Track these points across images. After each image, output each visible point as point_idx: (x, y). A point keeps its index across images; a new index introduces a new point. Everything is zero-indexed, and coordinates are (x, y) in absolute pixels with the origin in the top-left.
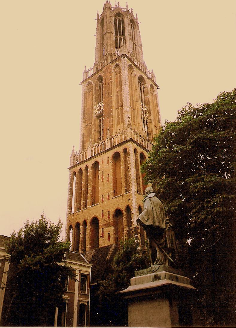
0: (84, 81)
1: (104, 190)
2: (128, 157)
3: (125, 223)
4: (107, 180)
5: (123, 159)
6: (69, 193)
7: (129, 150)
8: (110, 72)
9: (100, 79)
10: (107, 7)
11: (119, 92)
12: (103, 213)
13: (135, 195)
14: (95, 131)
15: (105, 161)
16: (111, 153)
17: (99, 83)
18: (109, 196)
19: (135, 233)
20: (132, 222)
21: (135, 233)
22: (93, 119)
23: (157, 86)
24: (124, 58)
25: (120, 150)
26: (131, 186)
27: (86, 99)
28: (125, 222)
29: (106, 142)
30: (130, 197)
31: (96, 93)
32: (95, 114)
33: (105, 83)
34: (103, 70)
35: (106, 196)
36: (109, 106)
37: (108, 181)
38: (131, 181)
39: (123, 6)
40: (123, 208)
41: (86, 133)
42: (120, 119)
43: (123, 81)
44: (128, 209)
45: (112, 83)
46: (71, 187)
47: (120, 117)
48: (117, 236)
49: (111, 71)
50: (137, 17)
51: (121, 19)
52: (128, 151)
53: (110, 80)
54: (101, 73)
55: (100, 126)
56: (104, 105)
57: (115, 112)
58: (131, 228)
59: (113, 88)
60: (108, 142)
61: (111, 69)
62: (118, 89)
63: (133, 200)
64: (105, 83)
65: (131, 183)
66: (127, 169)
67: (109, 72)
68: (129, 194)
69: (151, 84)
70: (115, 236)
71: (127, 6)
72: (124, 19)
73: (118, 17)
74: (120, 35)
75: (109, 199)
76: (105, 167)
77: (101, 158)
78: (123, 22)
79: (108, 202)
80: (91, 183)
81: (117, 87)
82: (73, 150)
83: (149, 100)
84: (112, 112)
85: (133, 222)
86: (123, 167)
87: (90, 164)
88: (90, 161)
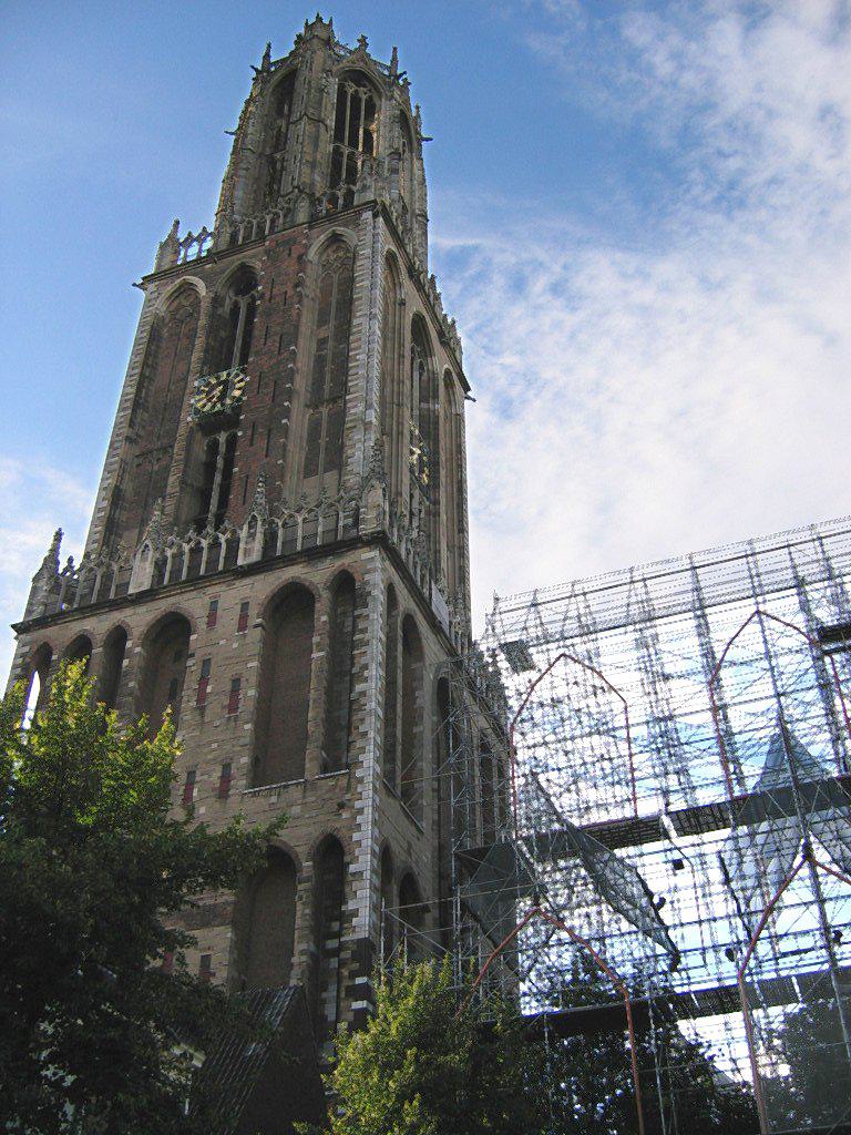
0: (159, 276)
1: (206, 750)
2: (356, 613)
3: (304, 915)
4: (227, 702)
5: (324, 618)
7: (367, 583)
8: (300, 258)
9: (244, 280)
10: (316, 36)
11: (331, 343)
13: (375, 790)
14: (183, 482)
15: (228, 619)
16: (260, 588)
17: (231, 293)
18: (226, 778)
19: (356, 966)
20: (346, 918)
21: (356, 966)
22: (182, 430)
23: (467, 388)
24: (375, 216)
25: (318, 575)
26: (359, 744)
27: (158, 347)
28: (302, 913)
29: (243, 534)
30: (348, 796)
31: (211, 331)
32: (197, 411)
33: (267, 296)
34: (267, 243)
36: (276, 387)
38: (362, 720)
39: (380, 55)
40: (300, 838)
41: (128, 487)
42: (322, 450)
43: (360, 298)
44: (333, 851)
45: (305, 301)
47: (323, 441)
48: (243, 977)
49: (306, 254)
50: (418, 116)
51: (364, 97)
52: (358, 585)
53: (297, 286)
54: (256, 259)
57: (298, 419)
58: (332, 944)
59: (303, 320)
60: (252, 536)
61: (307, 247)
62: (327, 331)
63: (360, 812)
64: (267, 296)
65: (362, 729)
66: (343, 670)
67: (294, 255)
68: (344, 781)
69: (446, 366)
70: (236, 975)
71: (394, 60)
72: (376, 99)
75: (223, 793)
76: (222, 642)
77: (207, 600)
78: (371, 110)
79: (217, 805)
80: (134, 707)
81: (322, 322)
82: (55, 551)
83: (437, 423)
84: (287, 413)
85: (355, 913)
86: (322, 654)
87: (138, 620)
88: (142, 609)
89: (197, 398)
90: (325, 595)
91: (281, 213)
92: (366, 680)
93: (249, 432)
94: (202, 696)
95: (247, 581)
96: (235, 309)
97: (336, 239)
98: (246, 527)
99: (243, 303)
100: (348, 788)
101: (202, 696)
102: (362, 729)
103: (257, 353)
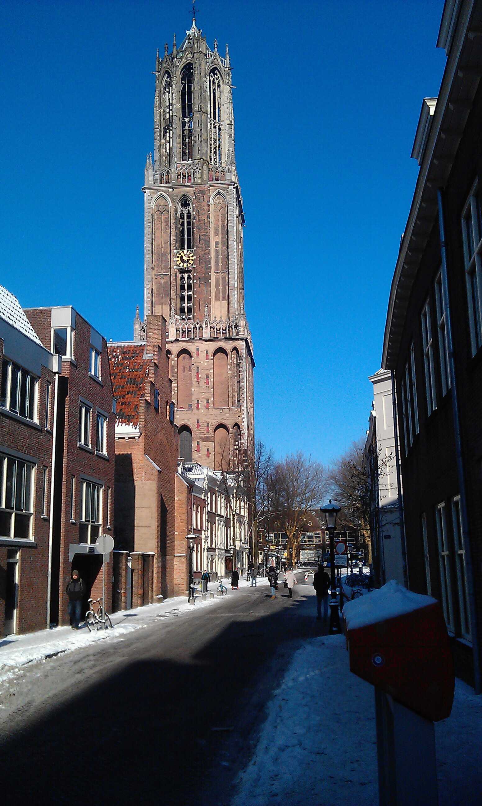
12: (198, 423)
15: (203, 355)
16: (213, 346)
25: (228, 346)
29: (204, 326)
35: (203, 403)
37: (207, 383)
40: (229, 423)
55: (182, 287)
56: (195, 257)
62: (219, 239)
74: (215, 118)
75: (208, 408)
79: (206, 410)
81: (216, 234)
88: (175, 345)
89: (177, 259)
94: (198, 378)
95: (207, 343)
96: (182, 214)
97: (219, 193)
99: (185, 212)
101: (198, 378)
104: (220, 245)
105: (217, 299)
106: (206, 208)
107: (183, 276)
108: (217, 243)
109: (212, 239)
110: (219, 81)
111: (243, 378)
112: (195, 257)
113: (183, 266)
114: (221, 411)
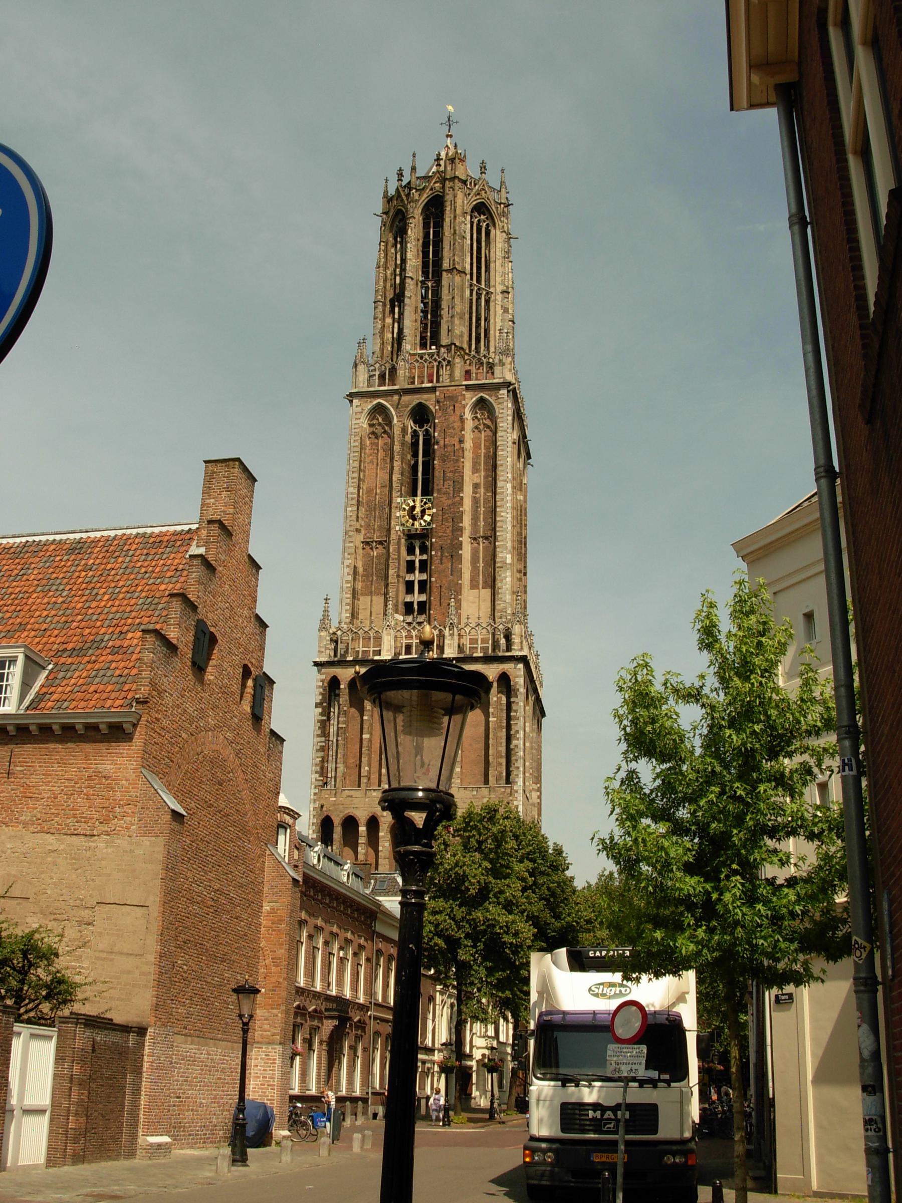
6: (319, 732)
7: (516, 683)
24: (509, 391)
26: (515, 773)
29: (447, 632)
38: (517, 760)
41: (360, 565)
46: (325, 718)
52: (512, 683)
56: (434, 510)
62: (480, 478)
68: (508, 790)
73: (476, 214)
81: (475, 470)
90: (495, 684)
91: (444, 363)
92: (518, 739)
93: (439, 554)
96: (415, 434)
98: (447, 629)
100: (511, 794)
102: (516, 765)
103: (439, 491)
104: (482, 490)
105: (474, 585)
106: (457, 424)
107: (412, 543)
108: (476, 486)
109: (467, 478)
110: (487, 225)
111: (517, 732)
112: (434, 510)
113: (413, 524)
114: (475, 793)
